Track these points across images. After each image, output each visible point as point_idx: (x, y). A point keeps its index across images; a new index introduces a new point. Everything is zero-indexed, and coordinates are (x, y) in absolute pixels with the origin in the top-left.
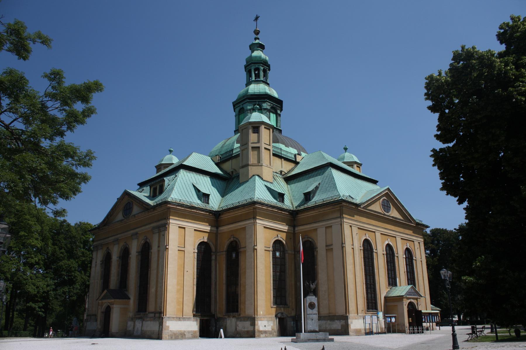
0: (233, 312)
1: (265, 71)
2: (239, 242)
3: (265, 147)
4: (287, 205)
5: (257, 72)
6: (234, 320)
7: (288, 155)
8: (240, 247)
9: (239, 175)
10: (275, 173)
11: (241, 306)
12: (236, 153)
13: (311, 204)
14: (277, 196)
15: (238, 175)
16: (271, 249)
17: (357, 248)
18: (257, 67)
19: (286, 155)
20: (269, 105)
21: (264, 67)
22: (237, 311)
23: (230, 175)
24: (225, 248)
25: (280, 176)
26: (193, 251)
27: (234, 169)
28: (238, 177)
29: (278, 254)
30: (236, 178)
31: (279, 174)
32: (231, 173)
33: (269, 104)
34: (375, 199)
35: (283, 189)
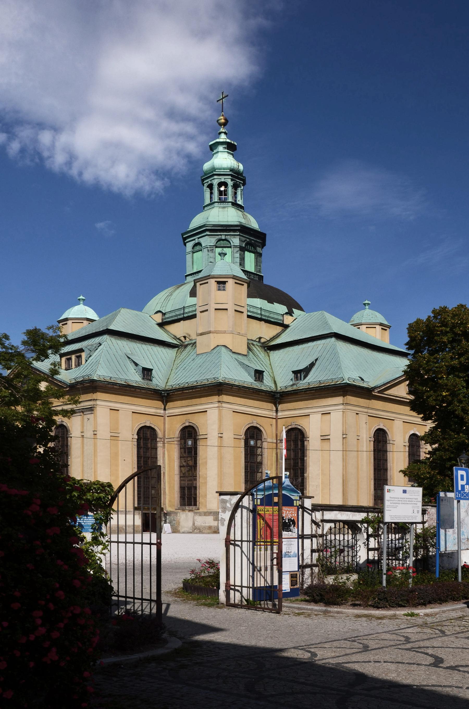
0: (190, 505)
1: (235, 187)
2: (198, 428)
3: (236, 309)
4: (268, 385)
5: (222, 189)
6: (190, 514)
7: (272, 315)
8: (198, 434)
9: (195, 343)
10: (251, 341)
11: (200, 500)
12: (189, 312)
13: (303, 384)
14: (253, 373)
15: (193, 342)
16: (243, 436)
17: (365, 440)
18: (223, 180)
19: (268, 317)
20: (243, 240)
21: (235, 180)
22: (195, 505)
23: (182, 341)
24: (177, 434)
25: (259, 344)
26: (131, 436)
27: (188, 334)
28: (194, 344)
29: (252, 443)
30: (191, 345)
31: (256, 341)
32: (183, 339)
33: (244, 239)
34: (399, 380)
35: (261, 362)
